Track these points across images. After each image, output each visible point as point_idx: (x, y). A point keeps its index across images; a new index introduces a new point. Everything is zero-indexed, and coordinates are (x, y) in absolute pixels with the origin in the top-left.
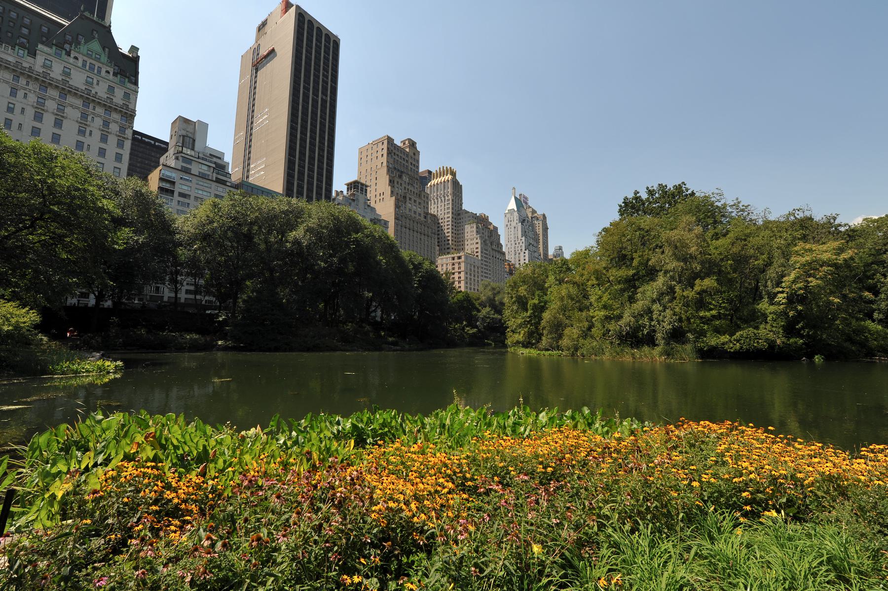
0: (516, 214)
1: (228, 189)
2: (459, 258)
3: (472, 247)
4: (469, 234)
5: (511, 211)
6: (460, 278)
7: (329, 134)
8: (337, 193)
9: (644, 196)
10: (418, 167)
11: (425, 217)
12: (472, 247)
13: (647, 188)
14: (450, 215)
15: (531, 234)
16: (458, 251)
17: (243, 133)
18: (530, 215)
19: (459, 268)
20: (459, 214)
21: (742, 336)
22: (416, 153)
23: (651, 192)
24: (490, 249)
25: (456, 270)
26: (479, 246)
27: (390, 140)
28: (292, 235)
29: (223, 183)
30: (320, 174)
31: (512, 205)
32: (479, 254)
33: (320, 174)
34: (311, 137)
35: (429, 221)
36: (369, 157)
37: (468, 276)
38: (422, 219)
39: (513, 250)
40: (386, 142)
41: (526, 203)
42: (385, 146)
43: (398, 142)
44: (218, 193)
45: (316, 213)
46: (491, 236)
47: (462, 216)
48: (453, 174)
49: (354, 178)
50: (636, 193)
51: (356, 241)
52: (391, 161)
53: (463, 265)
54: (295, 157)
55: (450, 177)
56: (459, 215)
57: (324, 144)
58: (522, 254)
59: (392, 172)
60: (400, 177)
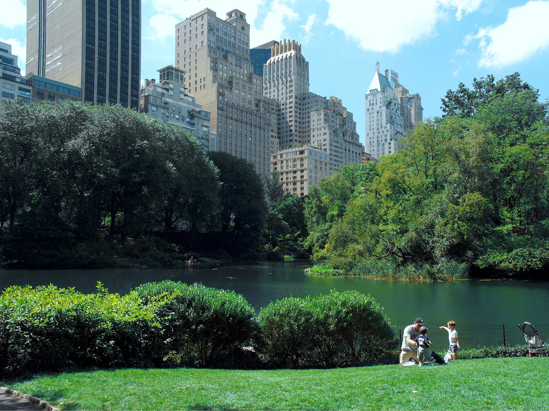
0: (379, 95)
1: (18, 85)
2: (302, 152)
3: (319, 138)
4: (316, 123)
5: (374, 92)
6: (302, 177)
7: (133, 14)
8: (148, 83)
9: (471, 88)
10: (248, 44)
11: (257, 105)
12: (319, 138)
13: (475, 79)
14: (293, 100)
15: (399, 120)
16: (302, 143)
17: (36, 17)
18: (399, 96)
19: (302, 165)
20: (304, 99)
21: (517, 254)
22: (245, 28)
23: (479, 85)
24: (341, 140)
25: (298, 167)
26: (327, 137)
27: (210, 13)
28: (71, 144)
29: (12, 79)
30: (125, 62)
31: (376, 84)
32: (327, 147)
33: (125, 62)
34: (111, 19)
35: (262, 109)
36: (188, 35)
37: (313, 175)
38: (253, 107)
39: (375, 140)
40: (206, 16)
41: (396, 81)
42: (205, 21)
43: (222, 16)
44: (6, 91)
45: (103, 115)
46: (344, 124)
47: (307, 101)
48: (298, 48)
49: (170, 61)
50: (462, 85)
51: (141, 151)
52: (213, 39)
53: (306, 162)
54: (94, 45)
55: (293, 52)
56: (305, 101)
57: (128, 27)
58: (387, 145)
59: (215, 53)
60: (225, 57)
